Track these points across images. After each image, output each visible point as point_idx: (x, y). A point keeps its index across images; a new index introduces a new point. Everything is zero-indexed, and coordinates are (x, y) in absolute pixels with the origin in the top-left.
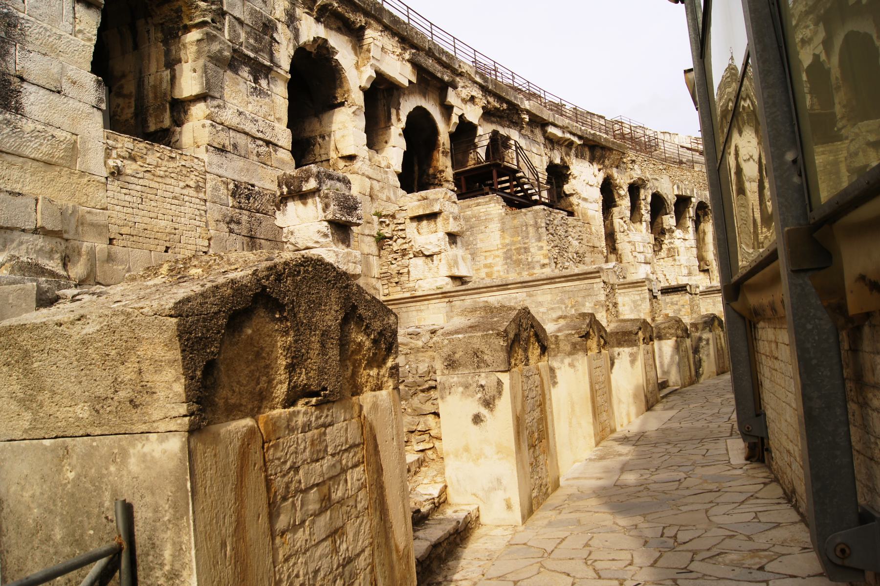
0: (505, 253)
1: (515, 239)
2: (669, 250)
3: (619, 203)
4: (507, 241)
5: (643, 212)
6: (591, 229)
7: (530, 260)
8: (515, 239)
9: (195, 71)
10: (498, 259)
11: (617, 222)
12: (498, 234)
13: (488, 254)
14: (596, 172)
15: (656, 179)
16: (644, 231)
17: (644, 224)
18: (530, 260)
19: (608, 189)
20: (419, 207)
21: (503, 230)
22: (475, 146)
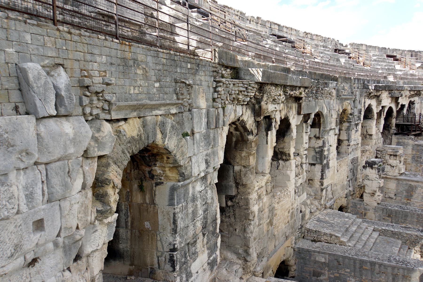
4: (414, 153)
12: (411, 150)
20: (392, 152)
21: (413, 149)
22: (403, 110)
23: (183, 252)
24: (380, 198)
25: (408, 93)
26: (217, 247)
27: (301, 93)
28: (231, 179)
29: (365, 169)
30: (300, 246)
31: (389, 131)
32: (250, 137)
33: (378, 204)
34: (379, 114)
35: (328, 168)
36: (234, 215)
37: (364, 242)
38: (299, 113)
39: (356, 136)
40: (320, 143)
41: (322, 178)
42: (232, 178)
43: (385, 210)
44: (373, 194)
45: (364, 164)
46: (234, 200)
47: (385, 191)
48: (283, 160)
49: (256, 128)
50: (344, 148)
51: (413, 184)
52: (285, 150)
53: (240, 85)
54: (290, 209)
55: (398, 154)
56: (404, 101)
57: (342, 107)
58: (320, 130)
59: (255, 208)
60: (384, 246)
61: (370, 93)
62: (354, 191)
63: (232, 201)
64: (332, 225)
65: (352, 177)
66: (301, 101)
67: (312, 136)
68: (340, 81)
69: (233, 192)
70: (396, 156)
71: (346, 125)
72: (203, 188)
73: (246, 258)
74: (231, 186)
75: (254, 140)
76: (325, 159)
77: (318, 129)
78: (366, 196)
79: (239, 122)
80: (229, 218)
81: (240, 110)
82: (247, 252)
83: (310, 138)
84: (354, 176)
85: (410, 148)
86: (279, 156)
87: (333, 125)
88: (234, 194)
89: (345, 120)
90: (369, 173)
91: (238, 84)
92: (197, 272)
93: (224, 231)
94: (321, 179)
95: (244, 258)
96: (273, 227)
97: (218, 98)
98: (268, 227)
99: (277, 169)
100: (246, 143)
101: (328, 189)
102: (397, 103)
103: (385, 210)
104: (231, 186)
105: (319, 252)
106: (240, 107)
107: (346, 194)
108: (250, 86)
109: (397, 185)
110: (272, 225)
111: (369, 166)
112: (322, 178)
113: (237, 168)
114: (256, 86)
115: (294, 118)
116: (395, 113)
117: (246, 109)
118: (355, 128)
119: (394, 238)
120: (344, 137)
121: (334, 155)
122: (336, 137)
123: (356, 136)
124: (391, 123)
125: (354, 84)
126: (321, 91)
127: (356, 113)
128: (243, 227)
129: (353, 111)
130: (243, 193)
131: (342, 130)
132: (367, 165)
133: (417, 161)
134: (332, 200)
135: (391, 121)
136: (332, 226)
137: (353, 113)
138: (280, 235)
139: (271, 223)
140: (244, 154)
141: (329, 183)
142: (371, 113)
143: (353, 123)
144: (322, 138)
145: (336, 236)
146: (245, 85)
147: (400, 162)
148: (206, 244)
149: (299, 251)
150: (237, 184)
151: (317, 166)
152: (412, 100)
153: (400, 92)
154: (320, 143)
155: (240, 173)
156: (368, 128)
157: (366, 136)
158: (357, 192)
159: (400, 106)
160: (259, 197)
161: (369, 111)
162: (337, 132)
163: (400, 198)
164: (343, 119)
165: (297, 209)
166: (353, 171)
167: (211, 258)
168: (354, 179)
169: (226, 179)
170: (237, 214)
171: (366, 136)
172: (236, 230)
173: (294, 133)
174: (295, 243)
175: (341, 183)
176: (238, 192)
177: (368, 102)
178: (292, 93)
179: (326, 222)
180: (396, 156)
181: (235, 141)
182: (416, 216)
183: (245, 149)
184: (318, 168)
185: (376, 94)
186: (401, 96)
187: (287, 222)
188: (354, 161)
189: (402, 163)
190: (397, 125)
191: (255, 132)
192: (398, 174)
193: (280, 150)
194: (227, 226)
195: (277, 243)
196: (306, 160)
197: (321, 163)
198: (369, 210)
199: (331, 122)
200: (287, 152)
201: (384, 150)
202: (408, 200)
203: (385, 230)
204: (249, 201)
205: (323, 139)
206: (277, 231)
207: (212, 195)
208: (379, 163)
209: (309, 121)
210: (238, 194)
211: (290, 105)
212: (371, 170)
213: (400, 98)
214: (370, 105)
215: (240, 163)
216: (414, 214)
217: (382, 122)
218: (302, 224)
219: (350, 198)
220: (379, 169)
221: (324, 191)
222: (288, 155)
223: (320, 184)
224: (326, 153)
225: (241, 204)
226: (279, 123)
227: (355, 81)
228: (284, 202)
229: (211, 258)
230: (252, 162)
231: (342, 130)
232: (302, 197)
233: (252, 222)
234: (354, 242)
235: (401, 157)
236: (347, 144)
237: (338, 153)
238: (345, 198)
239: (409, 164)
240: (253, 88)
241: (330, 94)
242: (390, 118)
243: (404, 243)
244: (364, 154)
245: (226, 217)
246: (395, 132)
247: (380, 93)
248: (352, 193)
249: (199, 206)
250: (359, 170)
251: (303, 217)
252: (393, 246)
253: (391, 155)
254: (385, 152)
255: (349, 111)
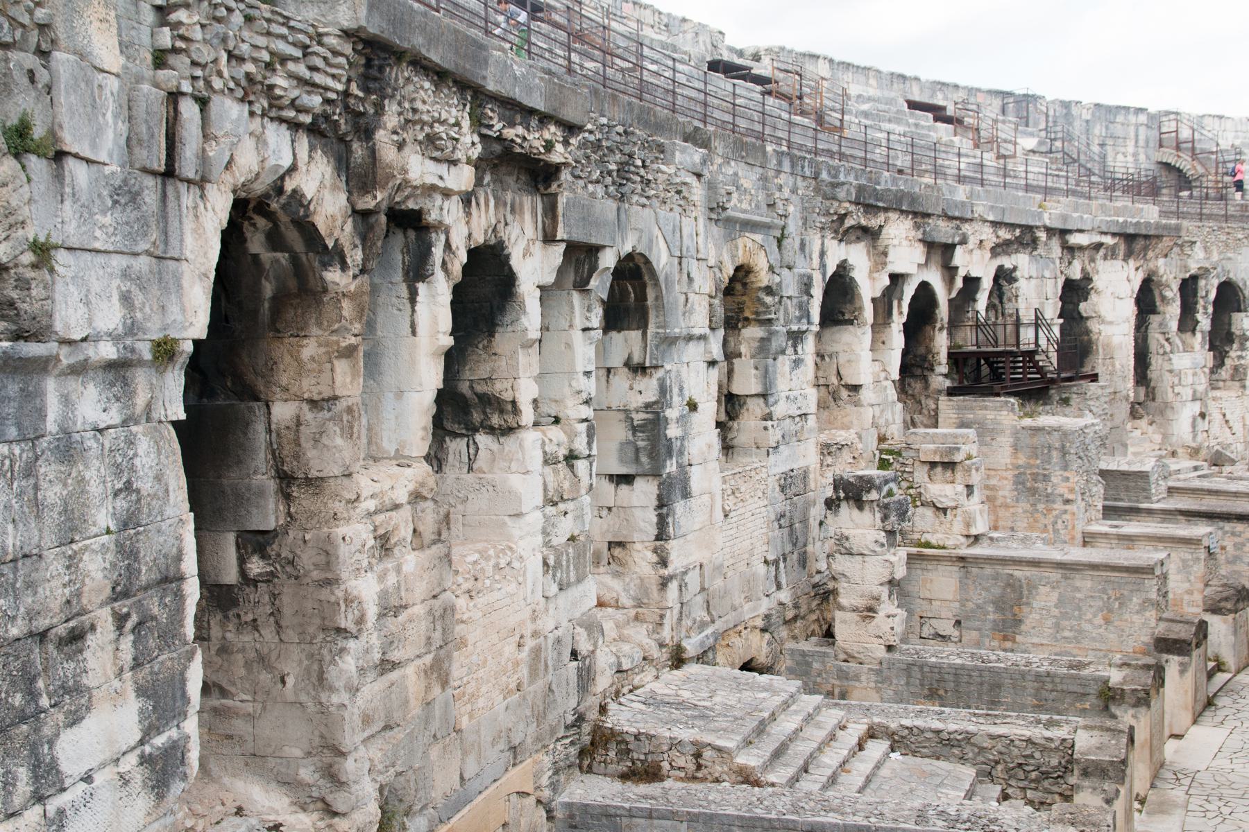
0: (1015, 476)
1: (1032, 462)
2: (1236, 369)
3: (1161, 308)
4: (1020, 462)
5: (1199, 317)
6: (1113, 366)
7: (1049, 491)
8: (1032, 462)
9: (756, 368)
10: (1005, 482)
11: (1155, 338)
12: (1008, 451)
13: (993, 473)
14: (1133, 272)
15: (1230, 259)
16: (1197, 347)
17: (1199, 335)
18: (1049, 491)
19: (1146, 301)
20: (935, 452)
21: (1016, 448)
22: (975, 300)
23: (18, 664)
24: (898, 624)
25: (989, 235)
26: (186, 700)
27: (549, 146)
28: (261, 459)
29: (836, 513)
30: (576, 799)
31: (925, 379)
32: (333, 276)
33: (890, 648)
34: (884, 305)
35: (686, 495)
36: (276, 613)
37: (829, 772)
38: (549, 238)
39: (796, 383)
40: (648, 389)
41: (662, 535)
42: (262, 455)
43: (916, 673)
44: (869, 611)
45: (829, 492)
46: (273, 550)
47: (918, 612)
48: (491, 430)
49: (358, 242)
50: (748, 424)
51: (1019, 573)
52: (499, 386)
53: (276, 29)
54: (528, 633)
55: (958, 457)
56: (975, 262)
57: (733, 257)
58: (644, 334)
59: (366, 588)
60: (907, 788)
61: (842, 218)
62: (796, 606)
63: (264, 556)
64: (704, 716)
65: (788, 548)
66: (554, 187)
67: (617, 360)
68: (720, 151)
69: (268, 515)
70: (950, 465)
71: (752, 333)
72: (114, 417)
73: (329, 798)
74: (261, 493)
75: (352, 288)
76: (670, 454)
77: (640, 332)
78: (844, 622)
79: (283, 200)
80: (256, 629)
81: (280, 147)
82: (334, 778)
83: (609, 370)
84: (795, 545)
85: (1005, 441)
86: (476, 417)
87: (699, 322)
88: (271, 524)
89: (747, 314)
90: (850, 525)
91: (269, 21)
92: (87, 778)
93: (233, 689)
94: (658, 538)
95: (320, 805)
96: (449, 691)
97: (175, 50)
98: (428, 688)
99: (470, 469)
100: (319, 302)
101: (687, 579)
102: (950, 271)
103: (916, 673)
104: (261, 493)
105: (650, 815)
106: (284, 133)
107: (767, 617)
108: (320, 44)
109: (963, 586)
110: (444, 683)
111: (847, 498)
112: (662, 535)
113: (282, 412)
114: (348, 49)
115: (527, 253)
116: (943, 311)
117: (312, 149)
118: (790, 351)
119: (947, 759)
120: (746, 382)
121: (709, 446)
122: (715, 374)
123: (796, 383)
124: (929, 350)
125: (779, 172)
126: (642, 172)
127: (791, 288)
128: (316, 667)
129: (777, 279)
130: (313, 515)
131: (739, 355)
132: (842, 495)
133: (1033, 491)
134: (709, 631)
135: (932, 339)
136: (703, 717)
137: (779, 284)
138: (486, 736)
139: (439, 672)
140: (310, 349)
141: (692, 559)
142: (852, 301)
143: (779, 328)
144: (656, 367)
145: (719, 750)
146: (301, 37)
147: (969, 487)
148: (132, 669)
149: (572, 816)
150: (285, 479)
151: (639, 483)
152: (1007, 262)
153: (958, 228)
154: (648, 389)
155: (297, 431)
156: (842, 359)
157: (838, 391)
158: (812, 611)
159: (959, 283)
160: (384, 545)
161: (840, 289)
162: (716, 351)
163: (975, 634)
164: (741, 310)
165: (558, 641)
166: (792, 529)
167: (160, 741)
168: (795, 556)
169: (239, 462)
170: (287, 611)
171: (838, 391)
172: (283, 682)
173: (531, 314)
174: (554, 787)
175: (742, 567)
176: (289, 514)
177: (837, 253)
178: (510, 133)
179: (681, 705)
180: (950, 465)
181: (274, 298)
182: (1030, 685)
183: (315, 330)
184: (644, 492)
185: (863, 222)
186: (964, 241)
187: (513, 686)
188: (791, 483)
189: (977, 496)
190: (957, 359)
191: (355, 256)
192: (963, 540)
193: (480, 388)
194: (248, 665)
195: (471, 770)
196: (590, 444)
197: (655, 474)
198: (857, 678)
199: (692, 305)
200: (507, 396)
201: (909, 447)
202: (1005, 638)
203: (910, 729)
204: (336, 547)
205: (660, 373)
206: (471, 717)
207: (161, 466)
208: (886, 482)
209: (593, 283)
210: (288, 524)
211: (509, 197)
212: (856, 512)
213: (959, 251)
214: (843, 267)
215: (294, 389)
216: (1023, 675)
217: (897, 339)
218: (581, 709)
219: (784, 632)
220: (886, 506)
221: (673, 586)
222: (509, 407)
223: (655, 558)
224: (673, 432)
225: (307, 559)
226: (464, 258)
227: (780, 163)
228: (497, 595)
229: (160, 741)
230: (344, 385)
231: (739, 355)
232: (574, 592)
233: (352, 644)
234: (789, 772)
235: (968, 470)
236: (759, 413)
237: (728, 448)
238: (763, 630)
239: (1007, 506)
240: (336, 53)
241: (679, 192)
242: (928, 328)
243: (987, 775)
244: (829, 460)
245: (241, 626)
246: (948, 383)
247: (881, 218)
248: (790, 614)
249: (94, 488)
250: (814, 523)
251: (586, 678)
252: (941, 785)
253: (933, 465)
254: (912, 453)
255: (763, 278)
